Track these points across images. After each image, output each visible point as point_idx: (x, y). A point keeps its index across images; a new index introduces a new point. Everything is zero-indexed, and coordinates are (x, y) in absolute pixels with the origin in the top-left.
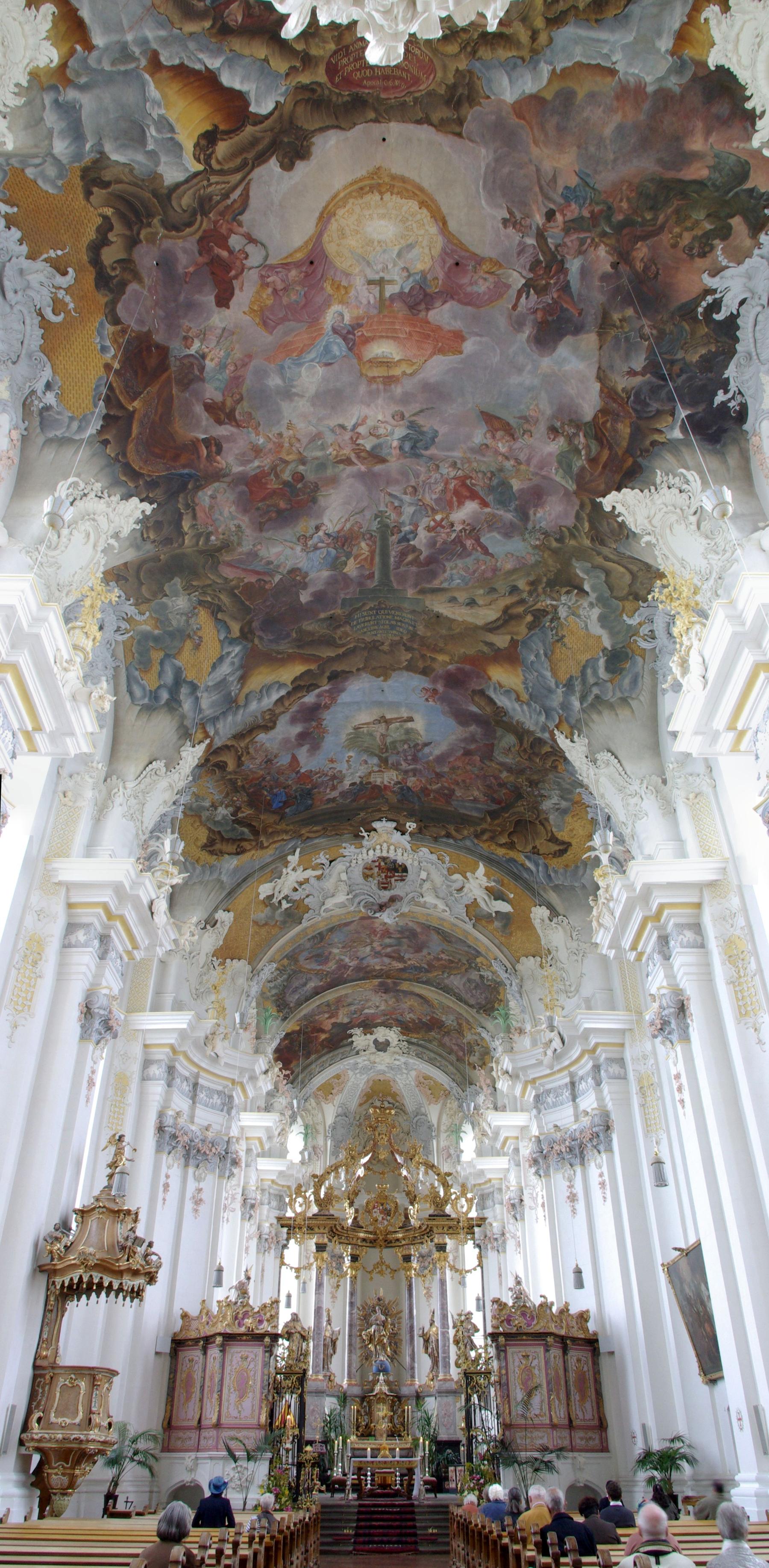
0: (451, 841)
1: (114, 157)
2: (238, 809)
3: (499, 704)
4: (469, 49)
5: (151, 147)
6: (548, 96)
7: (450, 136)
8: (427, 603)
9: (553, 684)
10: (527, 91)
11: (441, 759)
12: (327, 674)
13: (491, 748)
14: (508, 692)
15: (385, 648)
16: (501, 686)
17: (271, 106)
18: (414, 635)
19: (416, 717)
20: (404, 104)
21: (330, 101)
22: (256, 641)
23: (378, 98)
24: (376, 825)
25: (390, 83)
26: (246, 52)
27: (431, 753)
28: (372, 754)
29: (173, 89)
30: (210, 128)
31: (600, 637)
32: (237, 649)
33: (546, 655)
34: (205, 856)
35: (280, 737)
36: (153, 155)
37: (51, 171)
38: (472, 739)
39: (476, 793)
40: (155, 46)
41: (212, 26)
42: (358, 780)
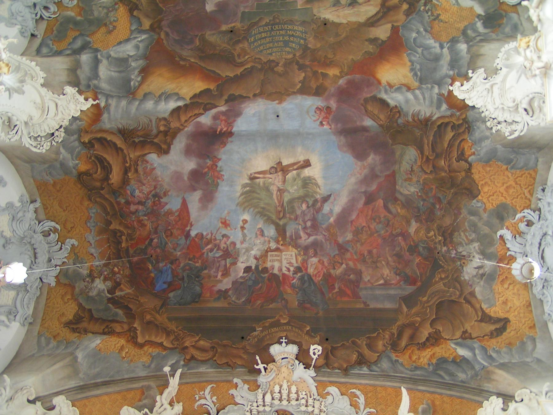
0: (365, 370)
2: (117, 285)
3: (392, 103)
8: (315, 11)
9: (438, 50)
11: (343, 219)
12: (225, 97)
13: (392, 178)
14: (398, 89)
15: (280, 69)
16: (390, 86)
18: (305, 48)
19: (314, 160)
22: (163, 36)
24: (275, 350)
27: (331, 211)
28: (269, 220)
31: (471, 8)
32: (144, 37)
33: (426, 30)
34: (66, 333)
35: (173, 168)
38: (372, 176)
39: (386, 272)
42: (252, 263)
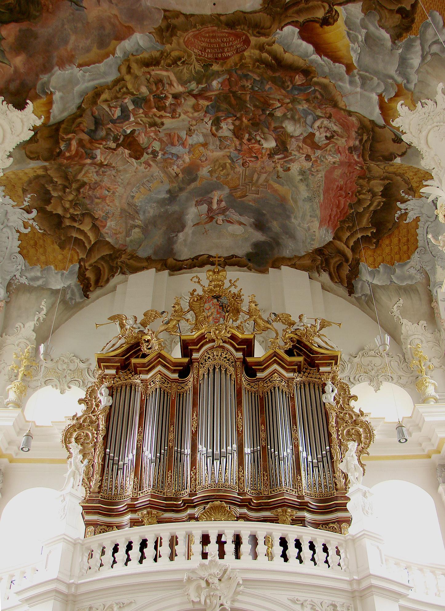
1: (387, 36)
4: (165, 54)
5: (364, 31)
6: (114, 42)
7: (171, 9)
10: (127, 41)
17: (286, 29)
20: (203, 24)
21: (248, 27)
23: (218, 27)
25: (211, 35)
26: (296, 58)
29: (343, 52)
30: (325, 27)
36: (364, 27)
37: (430, 33)
40: (347, 77)
41: (313, 77)
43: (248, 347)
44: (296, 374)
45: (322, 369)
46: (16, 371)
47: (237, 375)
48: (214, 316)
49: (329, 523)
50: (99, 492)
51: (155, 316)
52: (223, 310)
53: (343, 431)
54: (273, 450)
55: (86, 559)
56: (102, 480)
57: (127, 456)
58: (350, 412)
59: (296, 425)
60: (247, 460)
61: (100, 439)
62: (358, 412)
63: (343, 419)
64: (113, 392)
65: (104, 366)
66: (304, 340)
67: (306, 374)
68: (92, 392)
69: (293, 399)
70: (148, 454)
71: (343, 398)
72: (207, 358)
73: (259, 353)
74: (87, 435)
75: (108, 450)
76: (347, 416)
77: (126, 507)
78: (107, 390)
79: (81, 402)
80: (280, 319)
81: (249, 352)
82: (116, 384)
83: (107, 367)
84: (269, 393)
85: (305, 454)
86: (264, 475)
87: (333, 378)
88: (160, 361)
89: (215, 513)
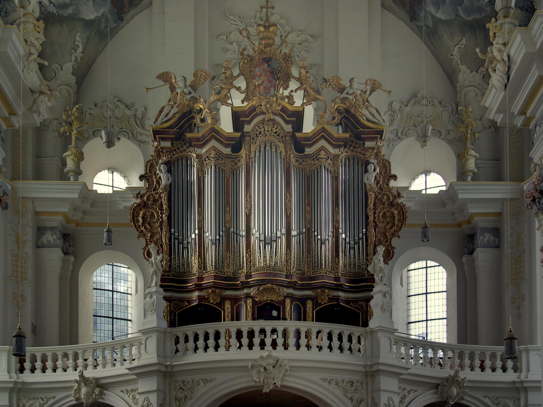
43: (297, 118)
44: (342, 149)
45: (368, 144)
46: (68, 134)
47: (286, 152)
48: (265, 85)
49: (358, 301)
50: (170, 271)
51: (205, 77)
52: (274, 78)
53: (379, 213)
54: (316, 234)
55: (173, 343)
56: (170, 260)
57: (191, 236)
58: (388, 193)
59: (338, 208)
60: (294, 241)
61: (165, 218)
62: (395, 192)
63: (381, 200)
64: (171, 167)
65: (159, 138)
66: (352, 111)
67: (352, 148)
68: (150, 167)
69: (337, 178)
70: (209, 235)
71: (383, 177)
72: (258, 133)
73: (309, 126)
74: (153, 214)
75: (173, 230)
76: (385, 197)
77: (194, 286)
78: (166, 168)
79: (142, 178)
80: (330, 84)
81: (298, 125)
82: (173, 158)
83: (163, 139)
84: (316, 173)
85: (344, 236)
86: (307, 256)
87: (377, 155)
88: (213, 135)
89: (267, 293)
